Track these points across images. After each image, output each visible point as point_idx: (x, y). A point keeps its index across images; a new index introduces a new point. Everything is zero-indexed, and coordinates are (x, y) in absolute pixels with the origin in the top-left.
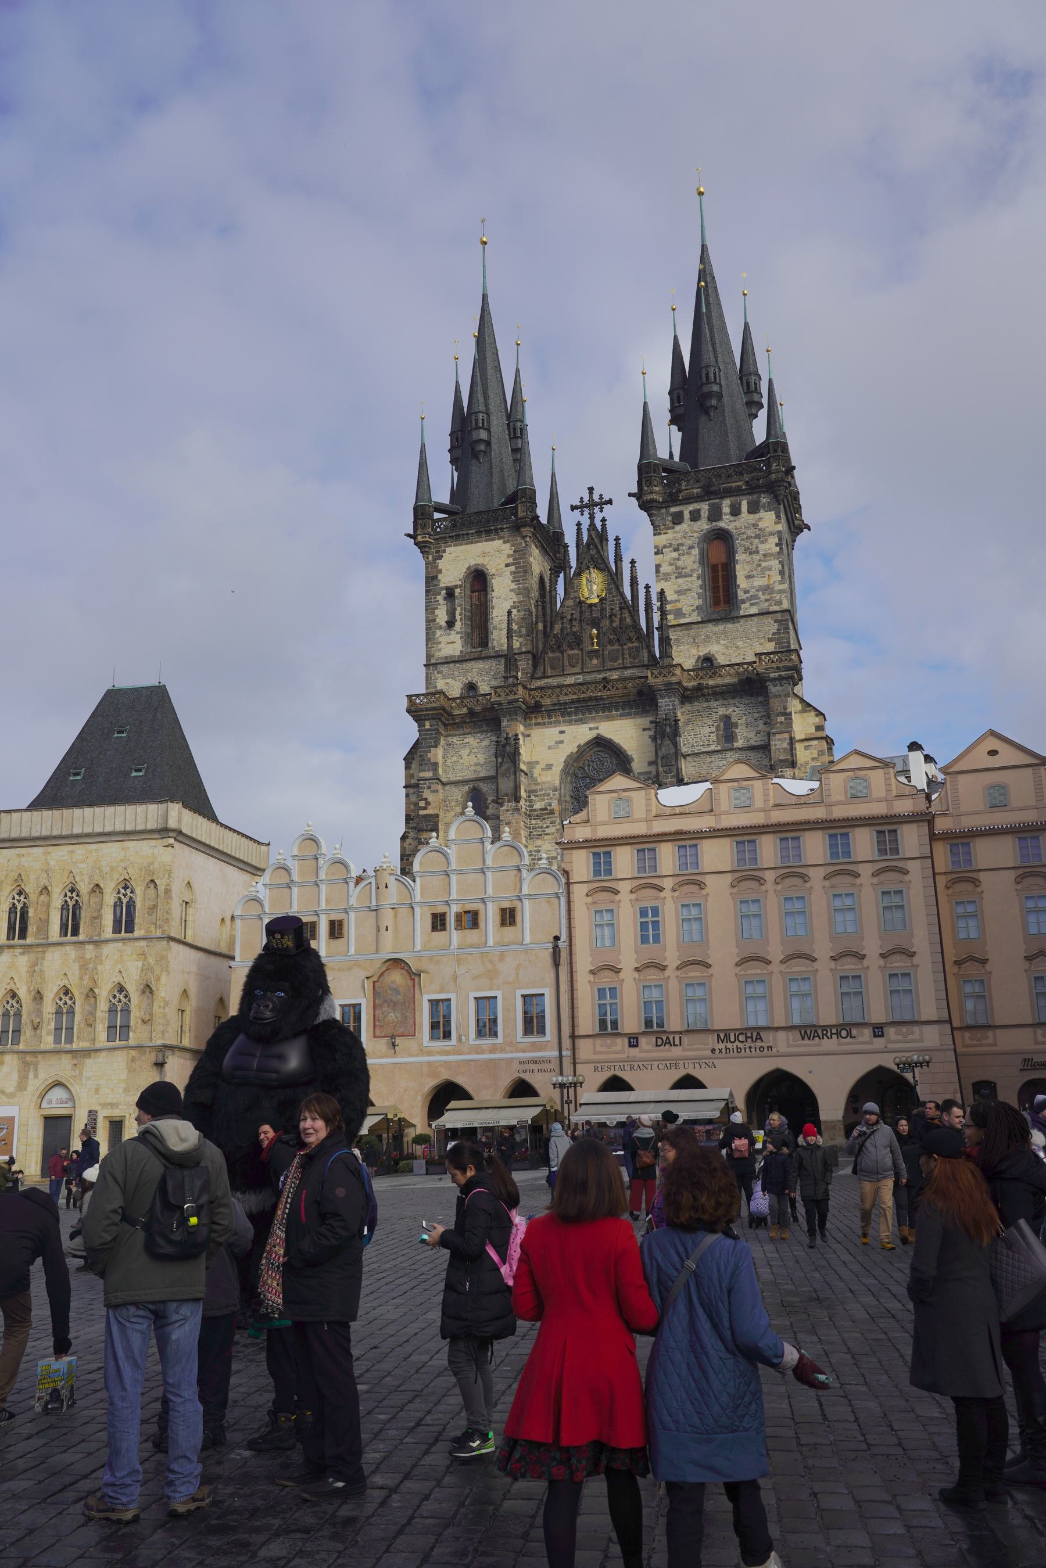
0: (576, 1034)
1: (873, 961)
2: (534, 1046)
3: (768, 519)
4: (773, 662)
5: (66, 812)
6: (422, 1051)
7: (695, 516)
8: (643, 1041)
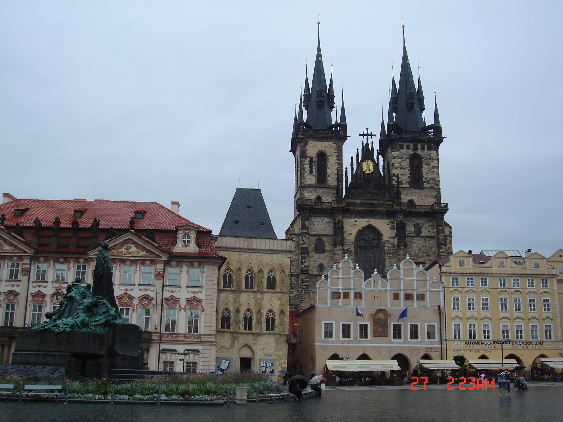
0: (447, 339)
2: (432, 343)
5: (250, 240)
7: (408, 147)
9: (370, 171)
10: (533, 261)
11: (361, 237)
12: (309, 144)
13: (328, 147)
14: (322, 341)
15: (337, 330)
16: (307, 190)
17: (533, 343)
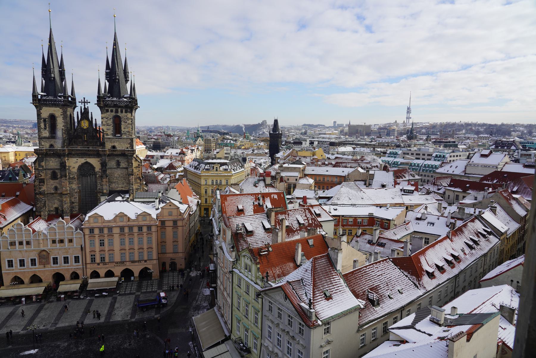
1: (145, 250)
2: (77, 266)
6: (51, 267)
7: (112, 111)
8: (100, 264)
11: (82, 169)
12: (43, 109)
13: (57, 112)
14: (7, 270)
15: (16, 263)
16: (43, 141)
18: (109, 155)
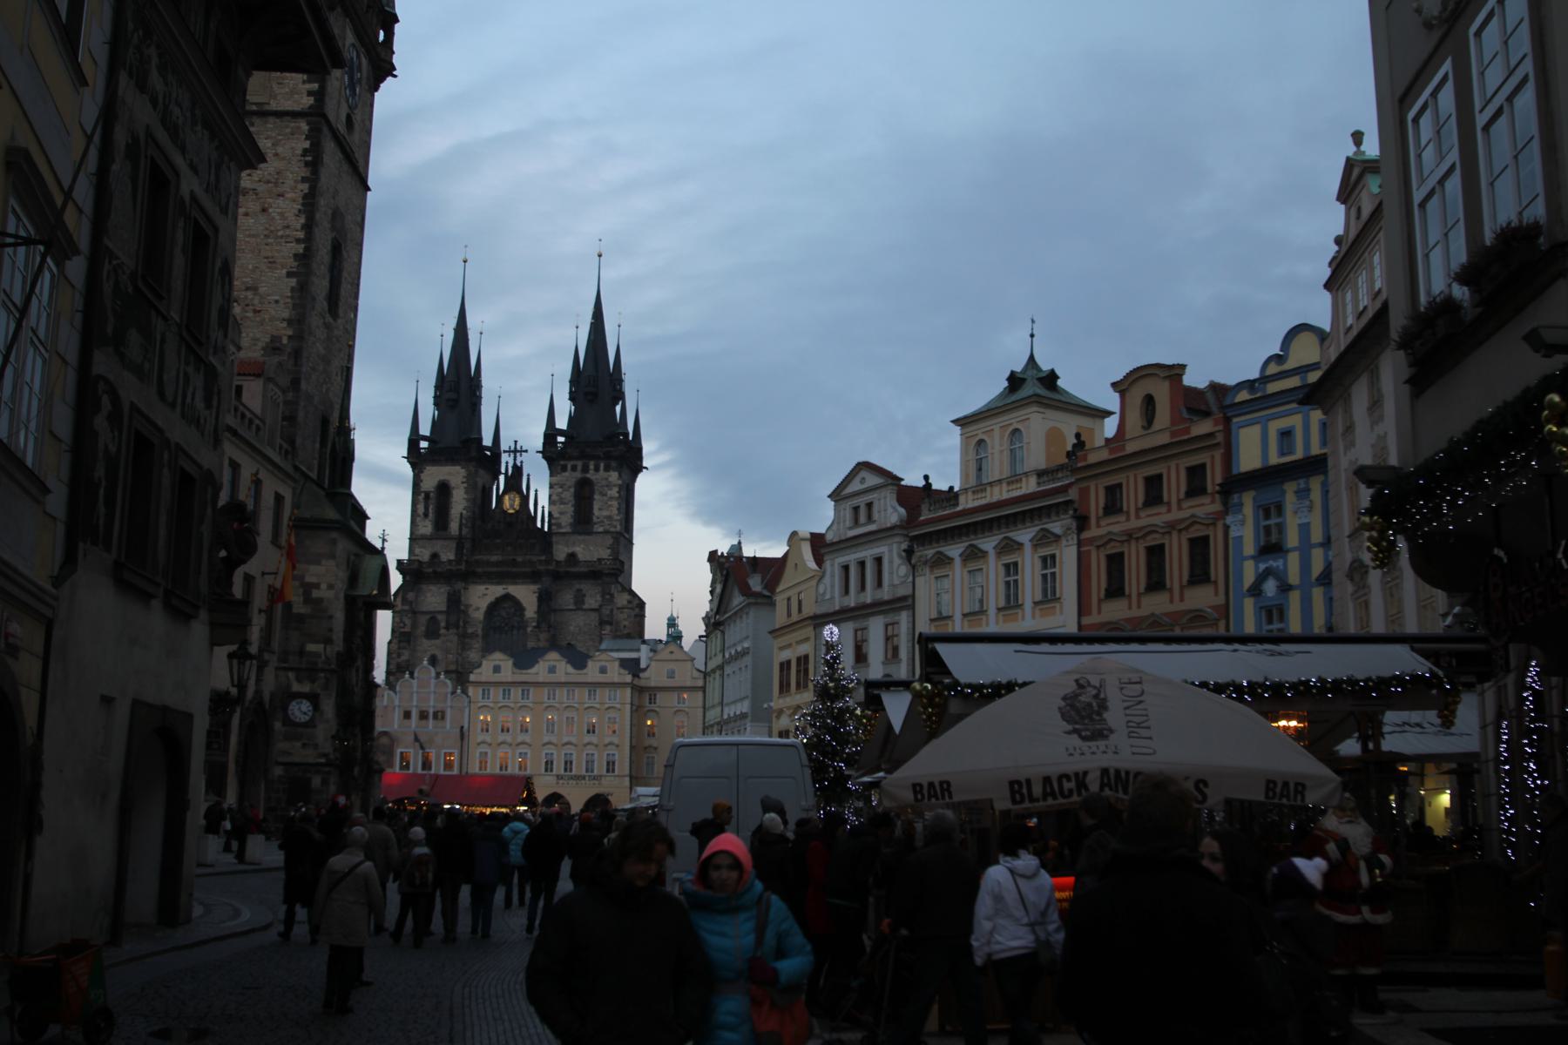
3: (614, 476)
4: (606, 564)
7: (574, 468)
9: (514, 509)
10: (598, 664)
13: (455, 475)
17: (587, 778)
18: (557, 576)
